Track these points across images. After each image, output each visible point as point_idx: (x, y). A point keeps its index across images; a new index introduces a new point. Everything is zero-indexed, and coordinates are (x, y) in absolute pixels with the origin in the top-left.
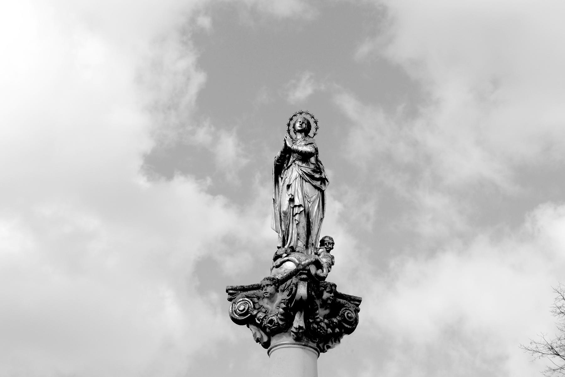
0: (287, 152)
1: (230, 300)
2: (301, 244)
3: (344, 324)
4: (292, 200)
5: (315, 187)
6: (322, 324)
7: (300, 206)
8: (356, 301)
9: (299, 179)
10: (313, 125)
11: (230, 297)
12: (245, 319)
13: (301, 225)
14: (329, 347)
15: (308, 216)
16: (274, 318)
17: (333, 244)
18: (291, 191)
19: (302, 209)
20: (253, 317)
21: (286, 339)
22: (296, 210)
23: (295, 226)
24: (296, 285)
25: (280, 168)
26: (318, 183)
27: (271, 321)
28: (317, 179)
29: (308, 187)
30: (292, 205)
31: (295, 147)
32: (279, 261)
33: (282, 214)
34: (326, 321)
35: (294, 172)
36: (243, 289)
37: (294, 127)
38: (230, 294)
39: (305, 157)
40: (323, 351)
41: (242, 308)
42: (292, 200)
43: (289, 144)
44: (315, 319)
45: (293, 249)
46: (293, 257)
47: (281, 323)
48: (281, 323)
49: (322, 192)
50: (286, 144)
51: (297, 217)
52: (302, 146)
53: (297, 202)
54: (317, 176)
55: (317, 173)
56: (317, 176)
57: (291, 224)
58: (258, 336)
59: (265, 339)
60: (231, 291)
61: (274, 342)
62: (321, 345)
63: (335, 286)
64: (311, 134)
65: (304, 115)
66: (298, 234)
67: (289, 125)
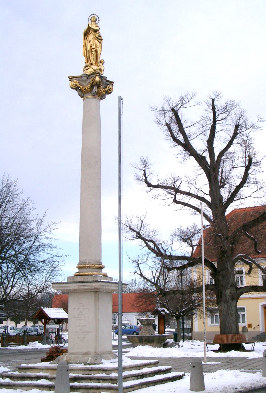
0: (89, 28)
1: (70, 81)
2: (94, 62)
3: (209, 164)
4: (91, 46)
5: (99, 42)
6: (102, 91)
7: (94, 49)
8: (112, 83)
9: (94, 39)
10: (98, 19)
11: (70, 79)
12: (76, 88)
13: (94, 55)
14: (103, 98)
15: (97, 52)
16: (86, 88)
17: (104, 62)
18: (91, 43)
19: (95, 50)
20: (78, 87)
21: (89, 95)
22: (93, 50)
23: (92, 56)
24: (95, 78)
25: (86, 34)
26: (100, 41)
27: (85, 89)
28: (100, 39)
29: (97, 42)
30: (91, 48)
31: (92, 27)
32: (87, 68)
33: (87, 51)
34: (103, 89)
35: (91, 37)
36: (76, 77)
37: (91, 19)
38: (70, 78)
39: (96, 31)
40: (102, 99)
41: (74, 84)
42: (91, 46)
43: (90, 26)
44: (100, 89)
45: (92, 64)
46: (92, 67)
47: (89, 90)
48: (89, 90)
49: (101, 44)
50: (89, 26)
51: (93, 52)
52: (94, 27)
53: (93, 47)
54: (100, 38)
55: (100, 37)
56: (100, 38)
57: (91, 55)
58: (80, 94)
59: (83, 95)
60: (70, 78)
61: (85, 95)
62: (101, 98)
63: (107, 78)
64: (97, 22)
65: (94, 15)
66: (93, 59)
67: (89, 18)
